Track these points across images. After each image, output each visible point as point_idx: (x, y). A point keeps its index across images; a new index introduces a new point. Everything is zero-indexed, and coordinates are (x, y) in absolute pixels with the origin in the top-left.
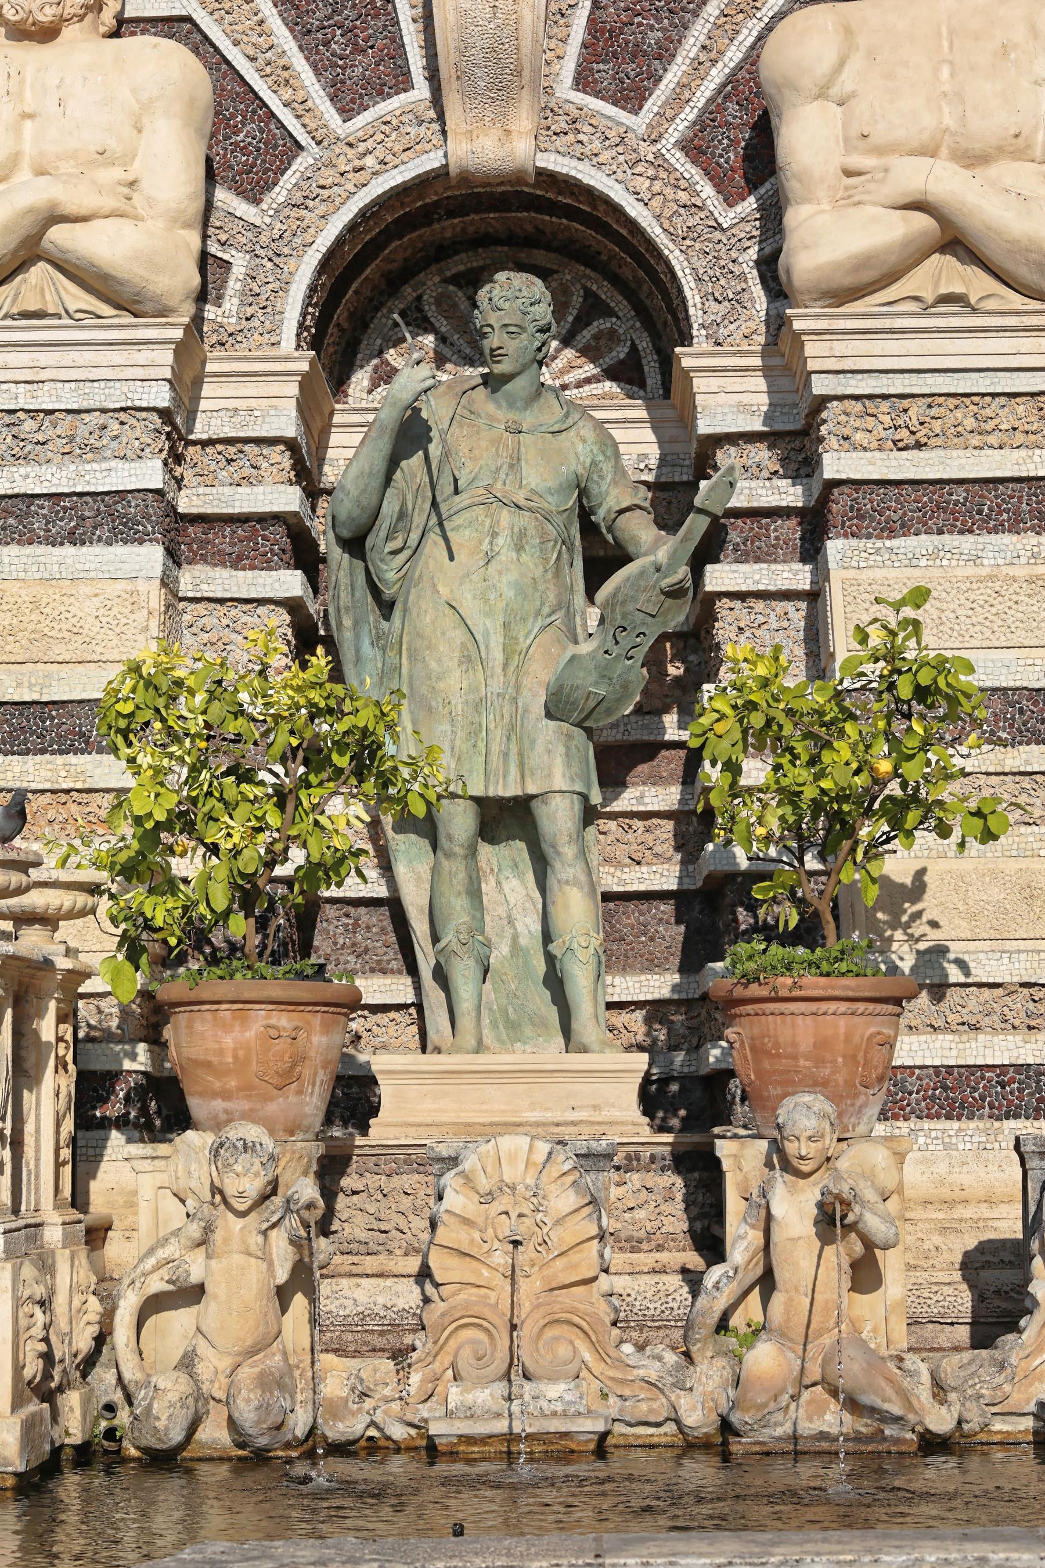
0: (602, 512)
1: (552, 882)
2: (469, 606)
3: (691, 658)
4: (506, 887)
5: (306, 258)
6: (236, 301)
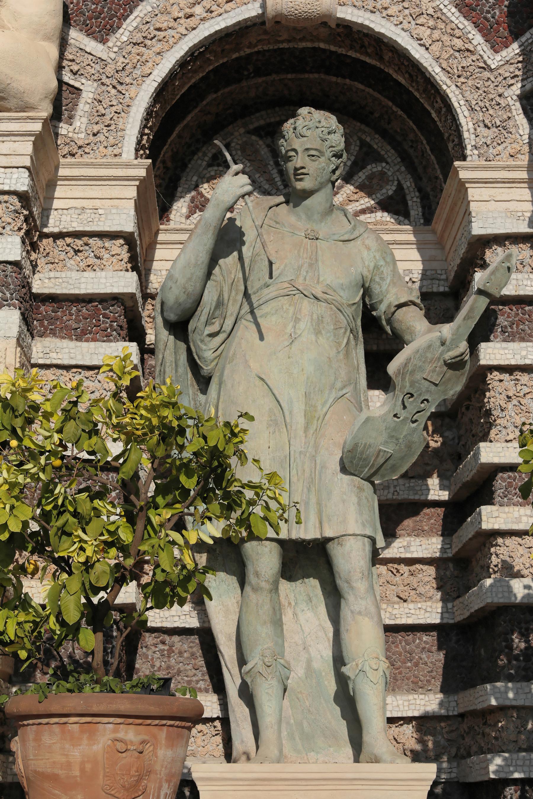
0: (383, 307)
1: (345, 612)
2: (276, 379)
3: (447, 434)
4: (302, 618)
5: (144, 86)
6: (85, 120)
